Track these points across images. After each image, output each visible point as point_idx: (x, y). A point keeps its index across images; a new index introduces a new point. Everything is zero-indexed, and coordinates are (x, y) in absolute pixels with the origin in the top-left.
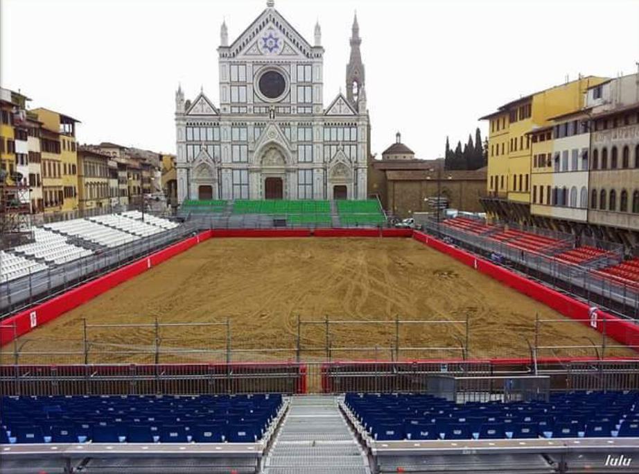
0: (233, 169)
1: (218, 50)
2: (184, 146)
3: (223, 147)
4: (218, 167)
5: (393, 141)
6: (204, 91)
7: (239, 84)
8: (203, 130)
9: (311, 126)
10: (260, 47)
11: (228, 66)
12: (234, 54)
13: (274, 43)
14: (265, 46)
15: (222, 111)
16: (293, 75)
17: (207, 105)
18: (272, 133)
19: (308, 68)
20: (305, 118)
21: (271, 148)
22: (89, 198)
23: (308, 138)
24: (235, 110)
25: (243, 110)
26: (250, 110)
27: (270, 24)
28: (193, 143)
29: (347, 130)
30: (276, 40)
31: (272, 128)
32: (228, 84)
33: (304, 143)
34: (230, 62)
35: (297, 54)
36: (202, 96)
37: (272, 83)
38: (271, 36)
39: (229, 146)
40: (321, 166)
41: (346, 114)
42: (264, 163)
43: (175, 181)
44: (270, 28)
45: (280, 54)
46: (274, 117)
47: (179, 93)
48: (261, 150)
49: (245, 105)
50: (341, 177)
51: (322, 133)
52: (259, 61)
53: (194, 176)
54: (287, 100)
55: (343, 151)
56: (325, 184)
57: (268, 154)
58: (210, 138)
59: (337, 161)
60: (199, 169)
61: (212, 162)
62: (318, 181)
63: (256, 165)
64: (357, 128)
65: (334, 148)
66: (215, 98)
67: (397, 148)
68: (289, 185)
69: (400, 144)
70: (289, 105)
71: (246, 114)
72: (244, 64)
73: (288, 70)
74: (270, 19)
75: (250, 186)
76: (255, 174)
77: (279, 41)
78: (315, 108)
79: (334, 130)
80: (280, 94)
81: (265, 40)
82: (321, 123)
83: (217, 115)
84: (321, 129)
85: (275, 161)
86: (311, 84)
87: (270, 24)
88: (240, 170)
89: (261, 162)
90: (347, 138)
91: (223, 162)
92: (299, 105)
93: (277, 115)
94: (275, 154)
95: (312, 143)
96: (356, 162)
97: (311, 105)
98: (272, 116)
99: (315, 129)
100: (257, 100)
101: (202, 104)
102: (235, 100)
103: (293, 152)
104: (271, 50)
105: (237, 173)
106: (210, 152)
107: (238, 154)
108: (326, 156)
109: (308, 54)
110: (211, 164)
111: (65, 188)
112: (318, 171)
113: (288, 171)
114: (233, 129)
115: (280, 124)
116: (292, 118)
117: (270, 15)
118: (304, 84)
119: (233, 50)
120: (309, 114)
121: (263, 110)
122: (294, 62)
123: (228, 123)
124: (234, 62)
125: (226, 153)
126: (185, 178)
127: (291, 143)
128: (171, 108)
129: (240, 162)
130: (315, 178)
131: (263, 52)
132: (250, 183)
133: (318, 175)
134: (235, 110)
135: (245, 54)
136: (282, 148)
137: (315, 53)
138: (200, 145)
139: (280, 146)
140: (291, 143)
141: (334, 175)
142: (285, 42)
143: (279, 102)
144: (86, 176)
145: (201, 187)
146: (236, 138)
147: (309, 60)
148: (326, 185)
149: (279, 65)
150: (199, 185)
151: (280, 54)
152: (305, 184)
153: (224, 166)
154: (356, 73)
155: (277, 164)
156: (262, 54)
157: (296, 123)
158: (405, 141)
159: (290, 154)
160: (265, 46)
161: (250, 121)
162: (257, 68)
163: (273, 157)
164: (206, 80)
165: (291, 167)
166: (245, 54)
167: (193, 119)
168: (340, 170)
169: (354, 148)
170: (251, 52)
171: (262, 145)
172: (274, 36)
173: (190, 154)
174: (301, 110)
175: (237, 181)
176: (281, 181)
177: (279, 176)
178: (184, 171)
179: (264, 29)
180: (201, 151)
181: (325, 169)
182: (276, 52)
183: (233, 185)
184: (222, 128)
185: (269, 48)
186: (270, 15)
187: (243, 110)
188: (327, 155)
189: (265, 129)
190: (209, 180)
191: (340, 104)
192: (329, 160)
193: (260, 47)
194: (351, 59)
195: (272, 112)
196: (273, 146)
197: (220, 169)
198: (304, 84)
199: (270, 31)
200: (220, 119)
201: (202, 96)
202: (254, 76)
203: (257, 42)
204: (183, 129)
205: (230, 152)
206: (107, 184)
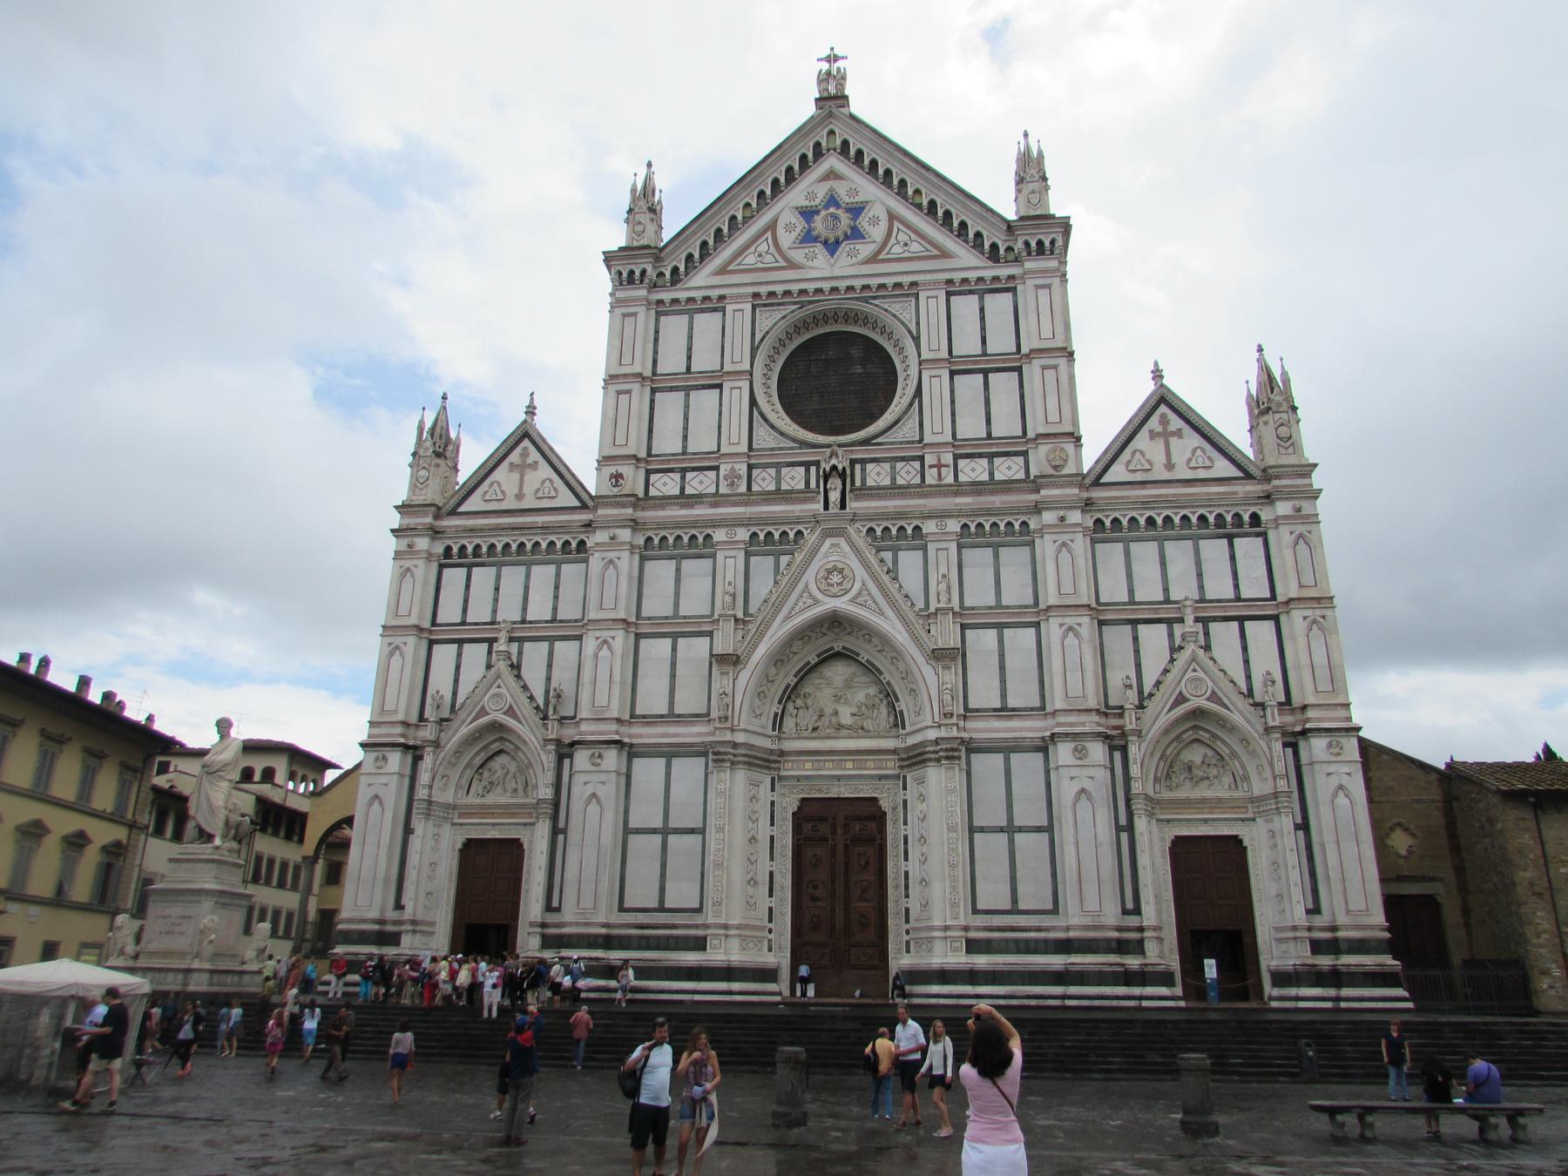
0: (632, 752)
2: (412, 646)
3: (590, 644)
4: (558, 742)
6: (542, 424)
7: (690, 383)
8: (513, 577)
9: (1025, 536)
10: (786, 239)
11: (644, 318)
12: (675, 270)
14: (808, 238)
16: (932, 329)
17: (545, 471)
18: (837, 575)
19: (999, 305)
20: (997, 500)
23: (1016, 592)
24: (666, 485)
25: (699, 483)
26: (733, 477)
27: (832, 162)
29: (1215, 549)
30: (856, 211)
31: (835, 552)
32: (636, 382)
33: (1000, 620)
34: (660, 302)
35: (945, 254)
36: (526, 435)
37: (836, 373)
38: (832, 201)
39: (620, 639)
41: (1202, 474)
42: (789, 723)
44: (832, 175)
46: (843, 506)
47: (437, 446)
48: (779, 658)
49: (709, 463)
50: (1204, 792)
51: (1083, 564)
52: (779, 289)
55: (1207, 648)
57: (814, 679)
58: (539, 609)
59: (1181, 699)
60: (474, 755)
61: (535, 718)
62: (1084, 806)
63: (751, 728)
64: (1264, 535)
65: (1154, 638)
66: (579, 440)
68: (923, 839)
71: (716, 499)
73: (908, 316)
74: (833, 135)
75: (712, 835)
76: (741, 775)
79: (1144, 553)
80: (874, 418)
81: (808, 214)
83: (584, 506)
84: (1080, 544)
85: (846, 719)
86: (1015, 364)
87: (832, 162)
88: (670, 753)
89: (778, 721)
90: (1219, 587)
91: (583, 714)
92: (963, 451)
94: (849, 684)
95: (1034, 616)
96: (1286, 704)
97: (1019, 447)
98: (834, 496)
99: (1046, 547)
100: (764, 438)
102: (669, 442)
103: (939, 656)
104: (832, 247)
106: (534, 674)
107: (674, 678)
108: (1116, 679)
109: (994, 246)
110: (528, 731)
112: (1080, 753)
113: (915, 758)
114: (649, 565)
115: (871, 530)
117: (832, 132)
120: (1008, 486)
121: (794, 479)
122: (934, 285)
123: (625, 535)
124: (675, 301)
125: (603, 675)
127: (928, 616)
128: (391, 477)
130: (1066, 790)
131: (798, 256)
132: (711, 821)
133: (1082, 774)
134: (666, 485)
135: (723, 270)
136: (886, 643)
137: (1034, 241)
138: (491, 641)
141: (1169, 770)
142: (892, 217)
143: (866, 442)
145: (472, 851)
146: (657, 604)
147: (1004, 272)
148: (1130, 828)
149: (866, 300)
153: (588, 730)
155: (860, 731)
156: (792, 265)
157: (954, 526)
159: (928, 674)
160: (808, 238)
162: (768, 320)
164: (546, 358)
165: (932, 735)
168: (1195, 755)
169: (1260, 633)
170: (750, 260)
171: (779, 631)
172: (846, 199)
173: (441, 681)
174: (974, 471)
175: (646, 813)
176: (879, 818)
180: (489, 667)
181: (1117, 743)
183: (628, 831)
184: (596, 562)
185: (825, 243)
186: (832, 132)
187: (699, 483)
189: (799, 557)
191: (1166, 435)
192: (1132, 696)
196: (833, 642)
197: (565, 751)
199: (827, 185)
201: (525, 434)
202: (754, 350)
203: (772, 226)
204: (424, 571)
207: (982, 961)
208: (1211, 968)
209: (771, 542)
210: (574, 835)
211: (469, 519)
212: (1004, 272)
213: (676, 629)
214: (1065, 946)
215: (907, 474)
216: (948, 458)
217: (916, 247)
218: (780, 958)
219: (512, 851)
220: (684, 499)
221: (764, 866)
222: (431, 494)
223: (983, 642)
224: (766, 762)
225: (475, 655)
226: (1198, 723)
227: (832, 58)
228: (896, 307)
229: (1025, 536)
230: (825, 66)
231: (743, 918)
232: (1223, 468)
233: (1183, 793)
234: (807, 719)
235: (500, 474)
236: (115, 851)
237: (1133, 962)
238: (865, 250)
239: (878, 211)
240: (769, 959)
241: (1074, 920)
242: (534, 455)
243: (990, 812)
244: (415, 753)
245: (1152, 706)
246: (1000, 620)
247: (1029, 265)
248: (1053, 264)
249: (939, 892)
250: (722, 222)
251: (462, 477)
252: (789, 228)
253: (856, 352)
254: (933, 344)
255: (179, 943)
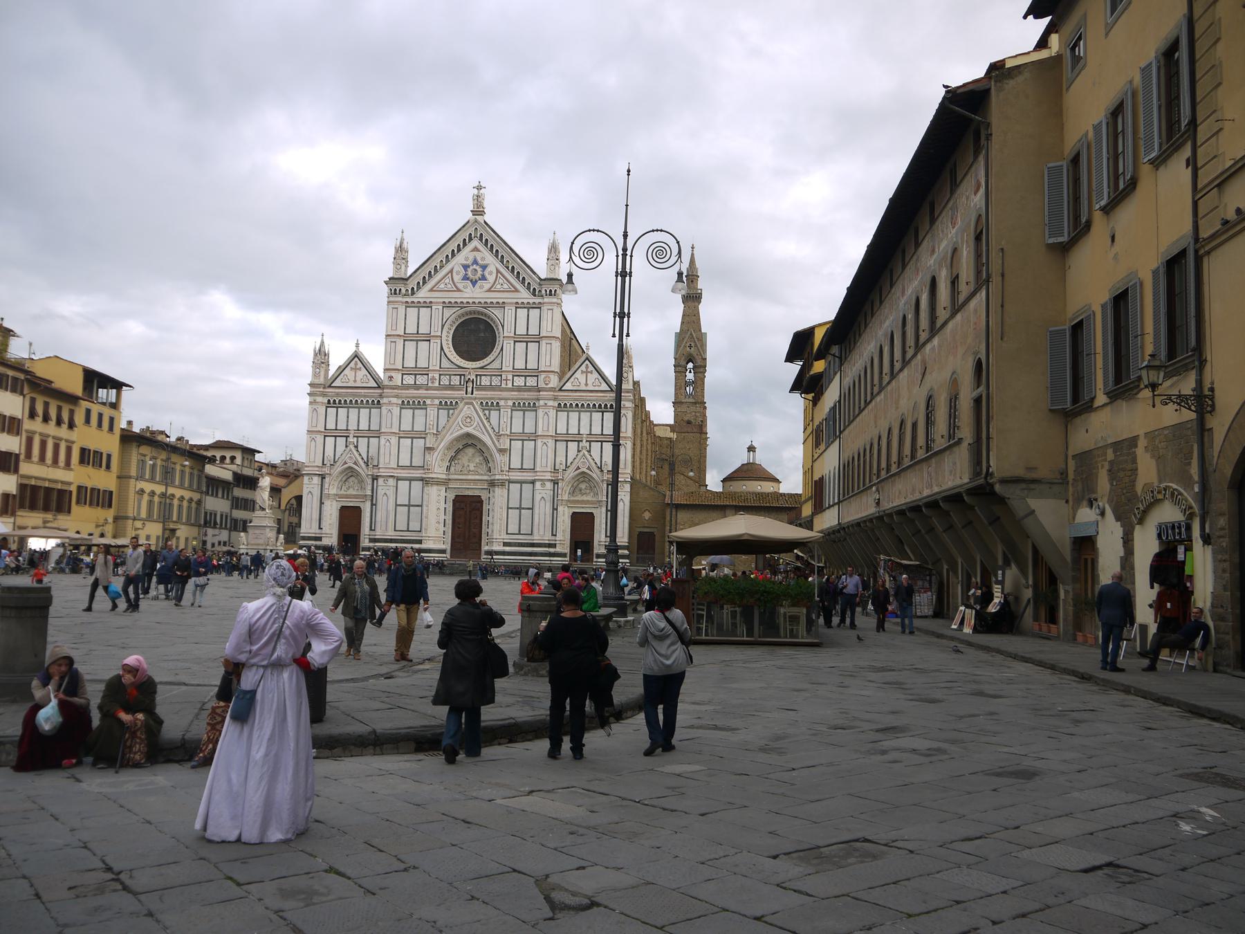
0: (398, 479)
1: (386, 283)
2: (320, 438)
3: (383, 441)
5: (742, 458)
8: (353, 413)
9: (534, 408)
10: (457, 278)
11: (402, 309)
13: (480, 272)
14: (466, 278)
15: (386, 383)
16: (511, 323)
18: (468, 419)
19: (534, 313)
20: (526, 395)
21: (466, 446)
22: (144, 515)
23: (529, 428)
24: (409, 380)
25: (421, 380)
28: (335, 434)
30: (484, 267)
31: (467, 410)
35: (516, 291)
37: (475, 336)
38: (475, 262)
39: (394, 440)
40: (548, 476)
43: (299, 499)
45: (489, 290)
48: (448, 449)
49: (425, 372)
53: (332, 489)
54: (496, 365)
56: (555, 509)
58: (364, 426)
65: (573, 446)
67: (749, 471)
69: (753, 464)
70: (499, 373)
72: (428, 305)
74: (477, 233)
76: (435, 487)
77: (488, 269)
78: (542, 376)
81: (466, 267)
82: (550, 403)
84: (552, 413)
85: (472, 468)
88: (411, 480)
89: (448, 468)
92: (517, 373)
93: (478, 389)
95: (534, 437)
98: (470, 390)
99: (540, 413)
100: (445, 364)
101: (355, 369)
102: (410, 363)
104: (474, 283)
105: (404, 485)
110: (362, 470)
111: (79, 488)
113: (492, 484)
116: (505, 394)
118: (527, 339)
119: (412, 284)
120: (530, 389)
121: (456, 381)
126: (317, 492)
127: (499, 436)
128: (305, 371)
129: (411, 467)
130: (538, 497)
131: (460, 286)
133: (544, 492)
134: (409, 380)
135: (431, 290)
139: (480, 440)
140: (499, 436)
141: (572, 493)
142: (498, 271)
144: (140, 477)
145: (343, 510)
146: (406, 426)
147: (537, 300)
150: (340, 505)
151: (489, 290)
152: (520, 508)
153: (383, 472)
154: (690, 347)
156: (459, 290)
157: (510, 403)
158: (760, 458)
160: (466, 278)
161: (433, 398)
163: (470, 460)
166: (431, 290)
167: (338, 394)
168: (583, 486)
170: (442, 286)
171: (449, 438)
174: (519, 382)
175: (403, 499)
177: (477, 493)
178: (316, 480)
179: (466, 251)
181: (555, 483)
182: (481, 287)
187: (421, 380)
188: (561, 458)
190: (356, 496)
193: (457, 278)
194: (682, 323)
195: (470, 384)
196: (469, 442)
197: (375, 478)
198: (527, 339)
200: (381, 396)
201: (356, 356)
203: (451, 271)
204: (322, 410)
205: (395, 451)
206: (199, 502)
207: (507, 549)
208: (579, 552)
209: (448, 406)
210: (379, 506)
211: (335, 390)
212: (537, 300)
213: (413, 435)
214: (533, 545)
215: (496, 381)
216: (510, 377)
217: (505, 286)
218: (448, 547)
219: (357, 511)
220: (416, 386)
221: (443, 517)
222: (321, 380)
223: (517, 445)
224: (445, 483)
225: (341, 441)
226: (583, 477)
227: (479, 188)
228: (496, 312)
229: (534, 408)
230: (476, 191)
231: (436, 535)
232: (604, 387)
233: (579, 498)
234: (459, 468)
235: (347, 371)
236: (199, 502)
237: (552, 550)
238: (487, 286)
239: (492, 268)
240: (443, 547)
241: (536, 538)
242: (360, 365)
243: (514, 503)
244: (323, 477)
245: (569, 470)
246: (525, 437)
247: (546, 300)
248: (555, 300)
249: (496, 527)
250: (430, 268)
251: (331, 373)
252: (458, 273)
253: (482, 327)
254: (508, 331)
255: (261, 541)
